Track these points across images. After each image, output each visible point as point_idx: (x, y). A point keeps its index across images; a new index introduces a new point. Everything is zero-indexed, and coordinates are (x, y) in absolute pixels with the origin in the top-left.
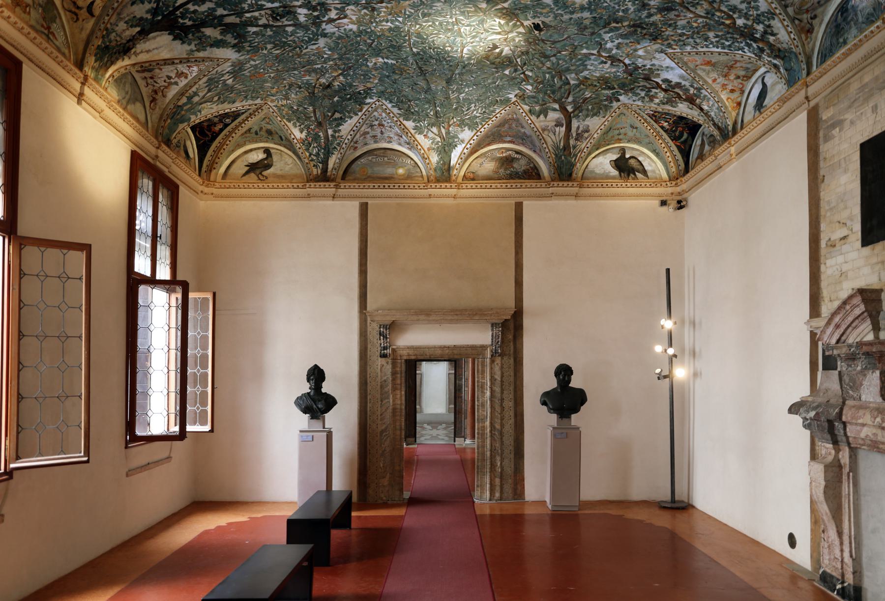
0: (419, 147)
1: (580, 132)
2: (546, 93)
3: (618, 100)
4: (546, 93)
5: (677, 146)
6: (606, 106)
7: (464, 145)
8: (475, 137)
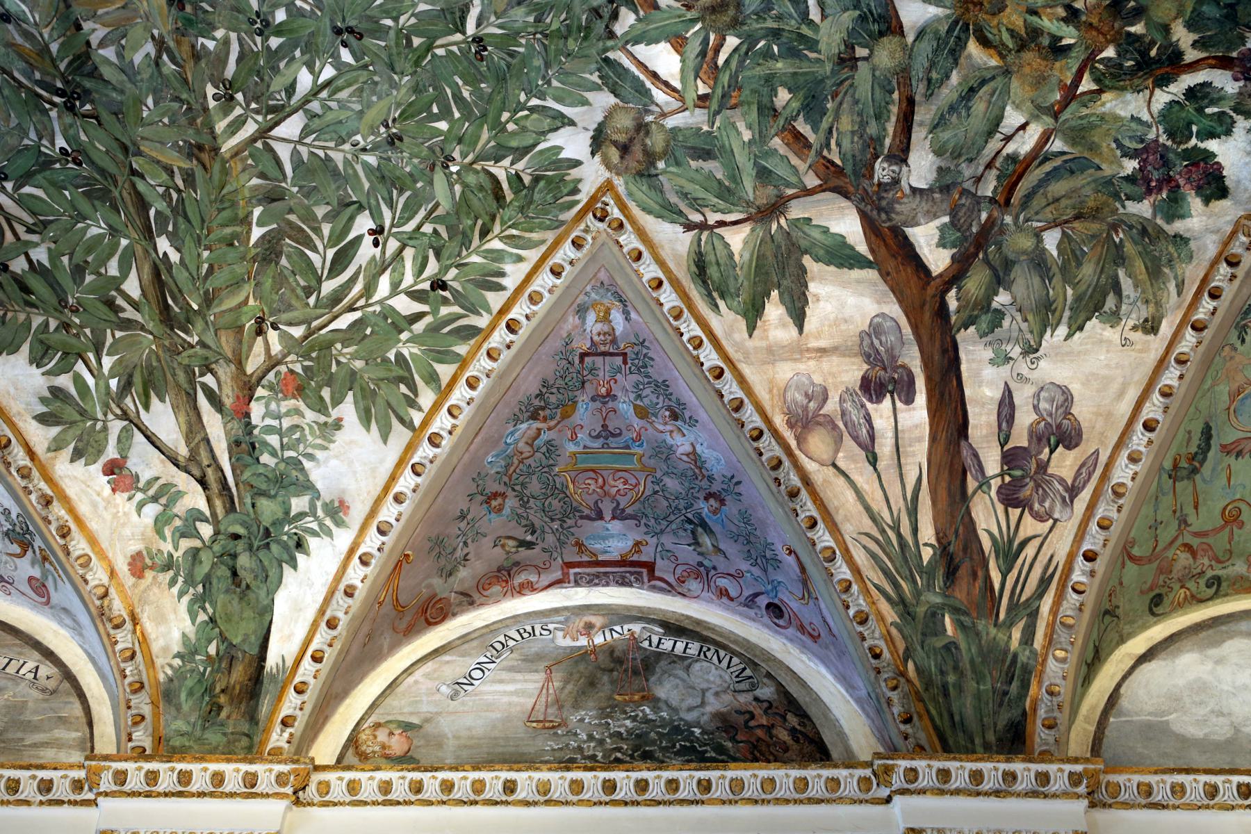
0: (79, 545)
1: (1020, 439)
2: (768, 111)
3: (1214, 185)
4: (768, 111)
6: (1145, 232)
7: (343, 538)
8: (407, 482)
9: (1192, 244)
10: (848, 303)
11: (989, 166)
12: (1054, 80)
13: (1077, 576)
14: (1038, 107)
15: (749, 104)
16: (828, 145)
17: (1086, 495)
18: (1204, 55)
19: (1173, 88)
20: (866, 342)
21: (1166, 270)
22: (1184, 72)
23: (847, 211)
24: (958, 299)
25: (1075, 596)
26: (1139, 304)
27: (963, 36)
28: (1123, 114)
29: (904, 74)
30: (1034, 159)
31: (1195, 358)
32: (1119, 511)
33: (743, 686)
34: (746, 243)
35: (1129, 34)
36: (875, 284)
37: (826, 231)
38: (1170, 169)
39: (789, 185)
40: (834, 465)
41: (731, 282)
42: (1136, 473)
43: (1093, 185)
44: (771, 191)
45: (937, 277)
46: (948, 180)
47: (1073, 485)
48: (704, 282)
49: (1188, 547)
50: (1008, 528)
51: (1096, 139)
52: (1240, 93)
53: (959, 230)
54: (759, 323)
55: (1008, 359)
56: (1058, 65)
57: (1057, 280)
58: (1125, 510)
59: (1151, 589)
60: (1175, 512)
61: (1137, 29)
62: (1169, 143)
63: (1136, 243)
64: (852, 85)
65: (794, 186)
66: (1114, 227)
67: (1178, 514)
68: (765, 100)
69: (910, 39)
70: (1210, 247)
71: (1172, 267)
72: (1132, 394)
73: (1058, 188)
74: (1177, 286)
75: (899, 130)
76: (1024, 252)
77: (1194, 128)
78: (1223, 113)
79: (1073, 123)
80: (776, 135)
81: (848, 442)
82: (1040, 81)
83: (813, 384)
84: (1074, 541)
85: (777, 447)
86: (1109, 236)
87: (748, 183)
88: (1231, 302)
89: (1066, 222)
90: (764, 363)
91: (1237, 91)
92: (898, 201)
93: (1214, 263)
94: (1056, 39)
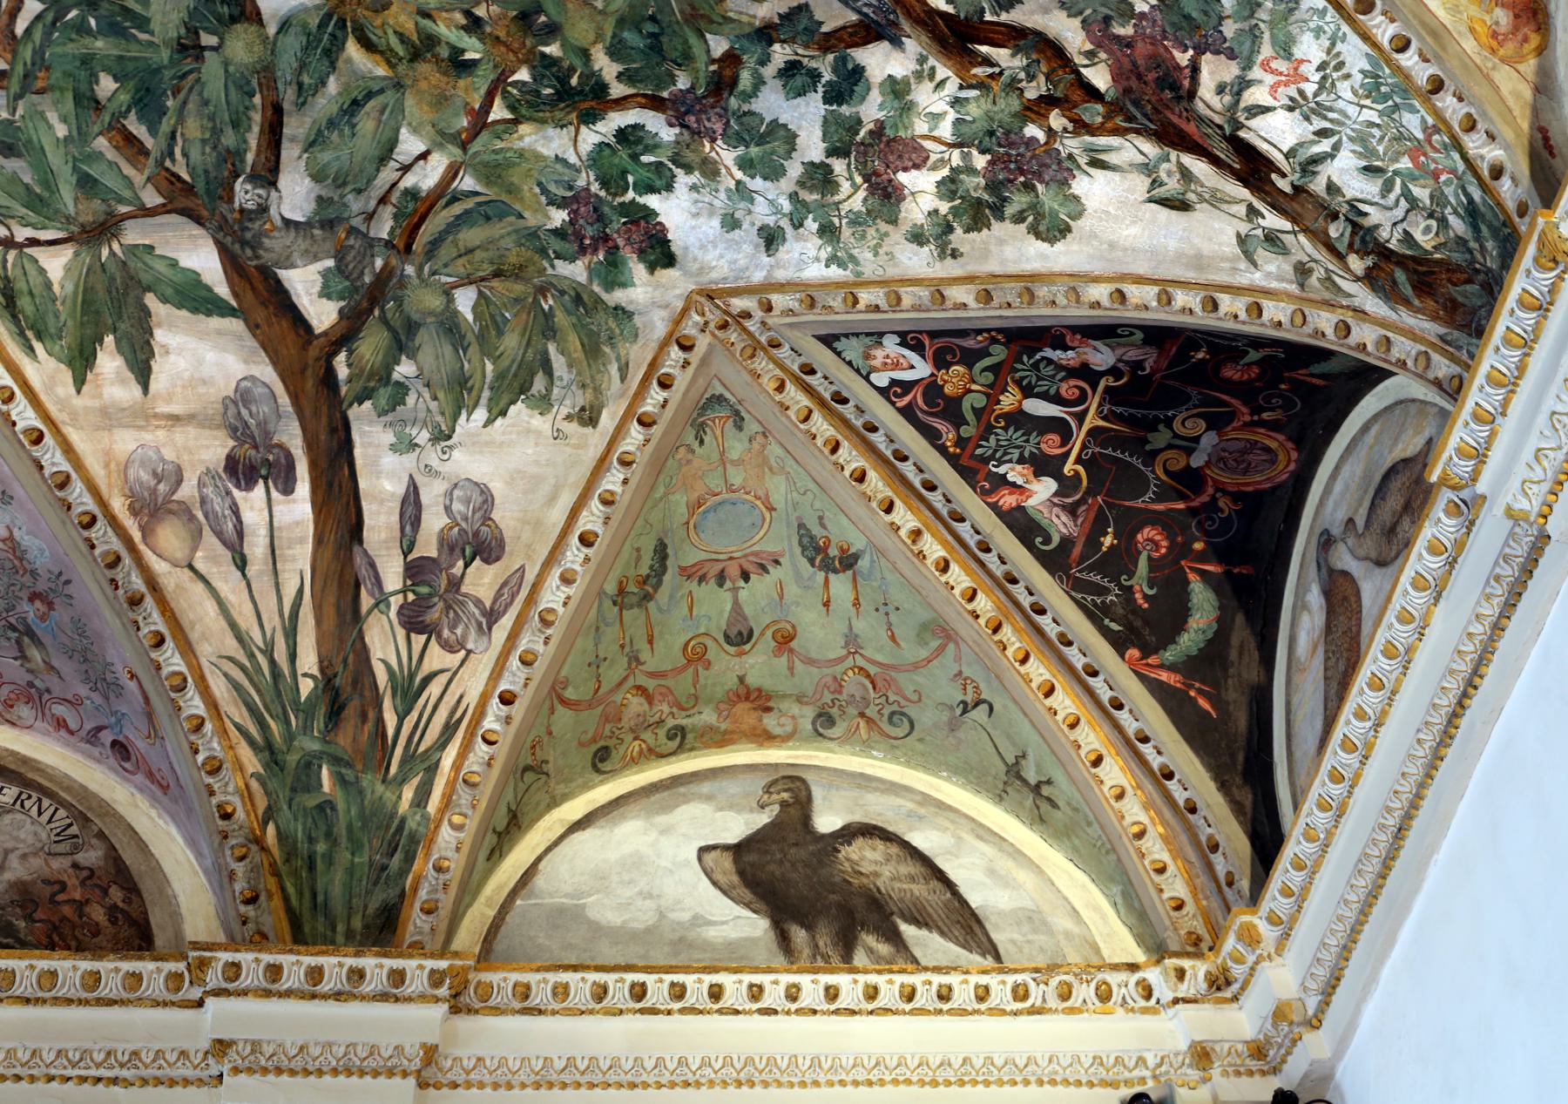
1: (427, 547)
2: (87, 102)
3: (660, 252)
4: (87, 102)
5: (1159, 691)
6: (579, 299)
9: (637, 320)
10: (204, 360)
11: (383, 200)
12: (459, 102)
13: (490, 723)
14: (442, 133)
15: (62, 90)
16: (171, 154)
17: (507, 622)
18: (632, 91)
19: (600, 126)
20: (232, 411)
21: (607, 350)
23: (201, 241)
24: (349, 366)
26: (574, 388)
27: (339, 34)
28: (545, 152)
29: (267, 73)
30: (440, 197)
31: (641, 459)
32: (546, 643)
33: (61, 848)
34: (68, 269)
35: (543, 55)
36: (240, 338)
37: (174, 264)
38: (606, 226)
39: (121, 200)
40: (191, 567)
41: (51, 321)
42: (568, 598)
43: (514, 237)
44: (97, 204)
45: (321, 335)
46: (331, 213)
47: (492, 609)
48: (14, 317)
49: (641, 690)
50: (410, 658)
51: (515, 180)
52: (677, 142)
53: (347, 278)
54: (89, 376)
55: (413, 446)
56: (462, 83)
57: (474, 350)
58: (553, 643)
59: (594, 740)
60: (622, 646)
61: (552, 50)
62: (603, 193)
63: (568, 312)
64: (198, 80)
65: (130, 203)
66: (542, 291)
67: (627, 649)
68: (83, 87)
69: (272, 30)
70: (658, 326)
71: (613, 346)
72: (567, 499)
73: (471, 236)
74: (620, 369)
75: (264, 144)
76: (432, 313)
77: (630, 179)
79: (486, 158)
80: (101, 133)
81: (209, 538)
82: (441, 101)
83: (163, 460)
85: (115, 539)
86: (535, 301)
87: (67, 194)
88: (685, 394)
89: (483, 279)
90: (98, 428)
91: (673, 138)
92: (266, 234)
93: (664, 345)
94: (457, 52)
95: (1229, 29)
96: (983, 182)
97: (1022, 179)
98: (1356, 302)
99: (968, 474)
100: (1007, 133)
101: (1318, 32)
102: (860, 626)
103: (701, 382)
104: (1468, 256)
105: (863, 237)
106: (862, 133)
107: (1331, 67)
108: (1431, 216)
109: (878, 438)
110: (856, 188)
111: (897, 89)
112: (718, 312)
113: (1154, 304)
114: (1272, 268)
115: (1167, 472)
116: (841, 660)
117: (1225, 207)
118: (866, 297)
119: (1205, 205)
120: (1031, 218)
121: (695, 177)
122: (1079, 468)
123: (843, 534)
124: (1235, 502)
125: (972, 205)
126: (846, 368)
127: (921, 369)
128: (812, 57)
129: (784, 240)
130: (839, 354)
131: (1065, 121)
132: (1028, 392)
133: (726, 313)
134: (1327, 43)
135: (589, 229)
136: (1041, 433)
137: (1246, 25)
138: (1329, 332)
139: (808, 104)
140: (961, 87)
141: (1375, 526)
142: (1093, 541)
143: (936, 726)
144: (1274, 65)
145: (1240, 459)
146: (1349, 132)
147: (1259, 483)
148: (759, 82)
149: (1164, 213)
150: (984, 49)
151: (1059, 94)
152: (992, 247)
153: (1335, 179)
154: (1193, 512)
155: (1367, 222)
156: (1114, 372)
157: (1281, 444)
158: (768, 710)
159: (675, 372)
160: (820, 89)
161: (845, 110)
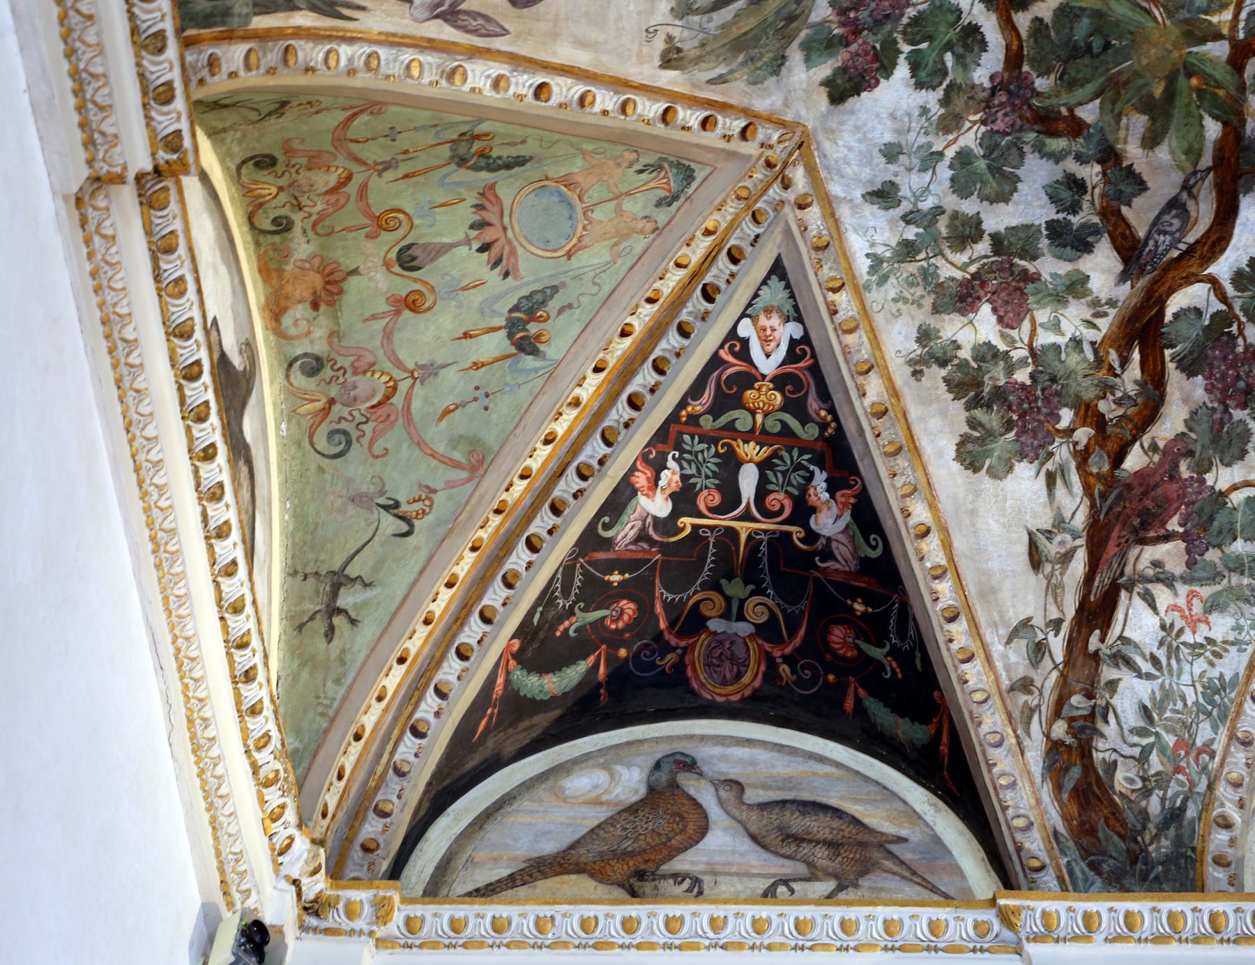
3: (843, 89)
9: (773, 79)
13: (345, 51)
17: (447, 33)
18: (1024, 34)
21: (741, 59)
22: (1000, 17)
25: (321, 56)
31: (630, 122)
32: (431, 83)
38: (870, 30)
47: (459, 12)
52: (973, 87)
60: (406, 152)
62: (905, 20)
63: (778, 13)
67: (401, 157)
70: (766, 100)
71: (744, 64)
72: (582, 59)
74: (721, 76)
77: (924, 46)
78: (946, 74)
84: (388, 34)
88: (698, 146)
91: (977, 81)
93: (745, 112)
95: (1213, 555)
96: (1001, 383)
97: (1015, 417)
98: (1027, 742)
99: (662, 435)
100: (1057, 394)
101: (1238, 628)
102: (451, 375)
103: (709, 157)
104: (1139, 827)
105: (912, 285)
106: (1022, 263)
107: (1213, 649)
108: (1144, 779)
109: (673, 340)
110: (963, 268)
111: (1076, 286)
112: (784, 156)
113: (929, 565)
114: (1013, 658)
115: (697, 604)
116: (399, 365)
117: (1050, 599)
118: (843, 299)
119: (1045, 582)
120: (977, 434)
121: (936, 110)
122: (688, 530)
123: (559, 336)
124: (673, 666)
125: (974, 378)
126: (750, 293)
127: (767, 365)
128: (1092, 203)
129: (887, 209)
130: (764, 282)
131: (1084, 441)
132: (764, 466)
133: (785, 165)
134: (1231, 638)
135: (866, 13)
136: (718, 487)
137: (1220, 568)
138: (984, 728)
139: (1042, 207)
140: (1093, 344)
141: (775, 816)
142: (611, 566)
143: (349, 481)
144: (1196, 601)
145: (726, 657)
146: (1167, 682)
147: (697, 678)
148: (1057, 157)
149: (1022, 548)
150: (1136, 355)
151: (1109, 430)
152: (935, 406)
153: (1121, 685)
154: (659, 636)
155: (1100, 725)
156: (811, 536)
157: (746, 686)
158: (315, 306)
159: (719, 130)
160: (1061, 216)
161: (1044, 243)
